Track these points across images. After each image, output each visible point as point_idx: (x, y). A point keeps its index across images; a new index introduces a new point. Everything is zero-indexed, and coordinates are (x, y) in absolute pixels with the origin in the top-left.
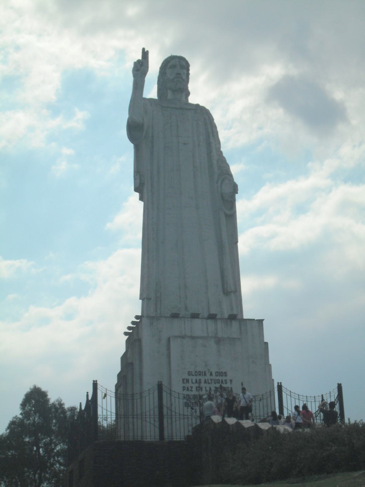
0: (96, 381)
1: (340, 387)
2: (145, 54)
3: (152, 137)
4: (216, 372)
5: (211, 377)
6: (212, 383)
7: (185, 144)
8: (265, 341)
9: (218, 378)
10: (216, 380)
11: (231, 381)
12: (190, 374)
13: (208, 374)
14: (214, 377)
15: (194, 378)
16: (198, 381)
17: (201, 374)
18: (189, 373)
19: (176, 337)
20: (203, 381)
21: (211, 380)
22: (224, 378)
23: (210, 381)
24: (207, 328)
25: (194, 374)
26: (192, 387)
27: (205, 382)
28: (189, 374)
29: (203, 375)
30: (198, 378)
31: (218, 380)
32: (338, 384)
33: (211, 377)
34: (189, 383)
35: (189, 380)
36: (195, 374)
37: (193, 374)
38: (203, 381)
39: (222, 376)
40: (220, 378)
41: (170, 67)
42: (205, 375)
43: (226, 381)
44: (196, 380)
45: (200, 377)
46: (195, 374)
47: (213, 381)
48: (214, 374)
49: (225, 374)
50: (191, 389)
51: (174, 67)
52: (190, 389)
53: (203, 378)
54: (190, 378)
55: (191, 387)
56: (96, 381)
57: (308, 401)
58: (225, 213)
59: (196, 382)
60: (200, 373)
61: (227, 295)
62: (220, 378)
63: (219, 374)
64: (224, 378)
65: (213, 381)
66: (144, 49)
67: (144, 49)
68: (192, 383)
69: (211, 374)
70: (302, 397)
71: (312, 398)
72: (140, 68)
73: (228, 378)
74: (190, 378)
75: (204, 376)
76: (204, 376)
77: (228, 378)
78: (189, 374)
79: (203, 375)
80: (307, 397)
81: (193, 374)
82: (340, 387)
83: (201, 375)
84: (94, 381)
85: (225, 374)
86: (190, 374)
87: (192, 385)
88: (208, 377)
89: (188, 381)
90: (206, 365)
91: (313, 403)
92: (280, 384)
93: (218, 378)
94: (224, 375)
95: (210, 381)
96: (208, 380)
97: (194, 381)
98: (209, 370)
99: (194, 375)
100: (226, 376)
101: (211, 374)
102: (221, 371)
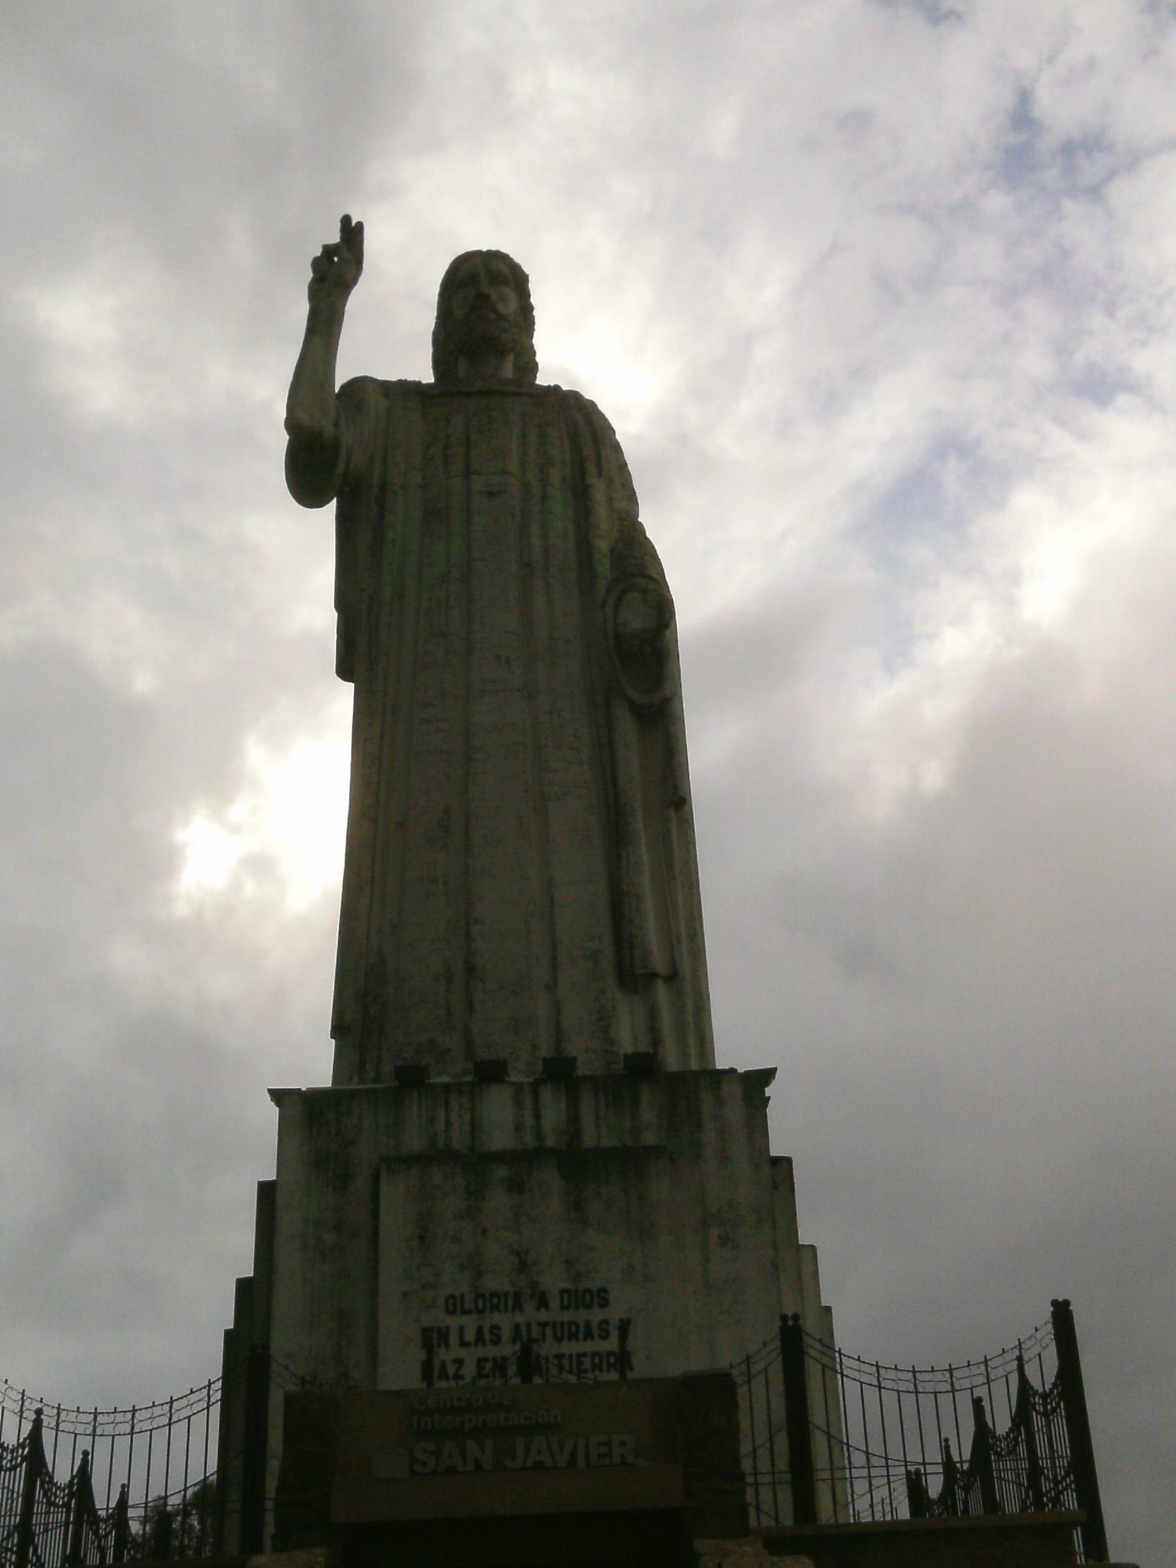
1: (1062, 1314)
3: (383, 488)
4: (564, 1292)
5: (543, 1316)
6: (544, 1339)
8: (776, 1150)
10: (562, 1324)
11: (624, 1327)
12: (454, 1305)
13: (529, 1306)
15: (470, 1324)
16: (487, 1336)
17: (498, 1305)
18: (451, 1301)
19: (405, 1161)
20: (506, 1335)
21: (543, 1325)
23: (536, 1332)
24: (537, 1116)
26: (460, 1362)
28: (451, 1308)
29: (510, 1308)
31: (571, 1323)
32: (1055, 1303)
33: (543, 1316)
34: (447, 1345)
35: (448, 1329)
36: (476, 1303)
38: (506, 1335)
39: (588, 1307)
40: (580, 1316)
43: (604, 1326)
44: (480, 1330)
45: (496, 1318)
46: (476, 1303)
47: (549, 1331)
48: (554, 1304)
49: (602, 1297)
50: (459, 1369)
52: (451, 1369)
53: (505, 1321)
54: (454, 1322)
55: (455, 1361)
57: (957, 1387)
59: (480, 1338)
60: (496, 1301)
62: (580, 1316)
63: (577, 1297)
64: (597, 1315)
65: (549, 1331)
66: (346, 220)
67: (346, 220)
68: (463, 1344)
70: (892, 1374)
75: (513, 1310)
76: (513, 1310)
78: (451, 1308)
79: (510, 1308)
80: (914, 1372)
81: (469, 1305)
82: (1062, 1314)
83: (502, 1307)
85: (602, 1297)
86: (454, 1304)
87: (463, 1353)
89: (444, 1335)
90: (523, 1267)
91: (945, 1400)
92: (790, 1323)
93: (568, 1316)
94: (596, 1300)
96: (529, 1326)
97: (470, 1336)
98: (533, 1285)
99: (469, 1312)
100: (605, 1303)
101: (542, 1303)
102: (582, 1286)
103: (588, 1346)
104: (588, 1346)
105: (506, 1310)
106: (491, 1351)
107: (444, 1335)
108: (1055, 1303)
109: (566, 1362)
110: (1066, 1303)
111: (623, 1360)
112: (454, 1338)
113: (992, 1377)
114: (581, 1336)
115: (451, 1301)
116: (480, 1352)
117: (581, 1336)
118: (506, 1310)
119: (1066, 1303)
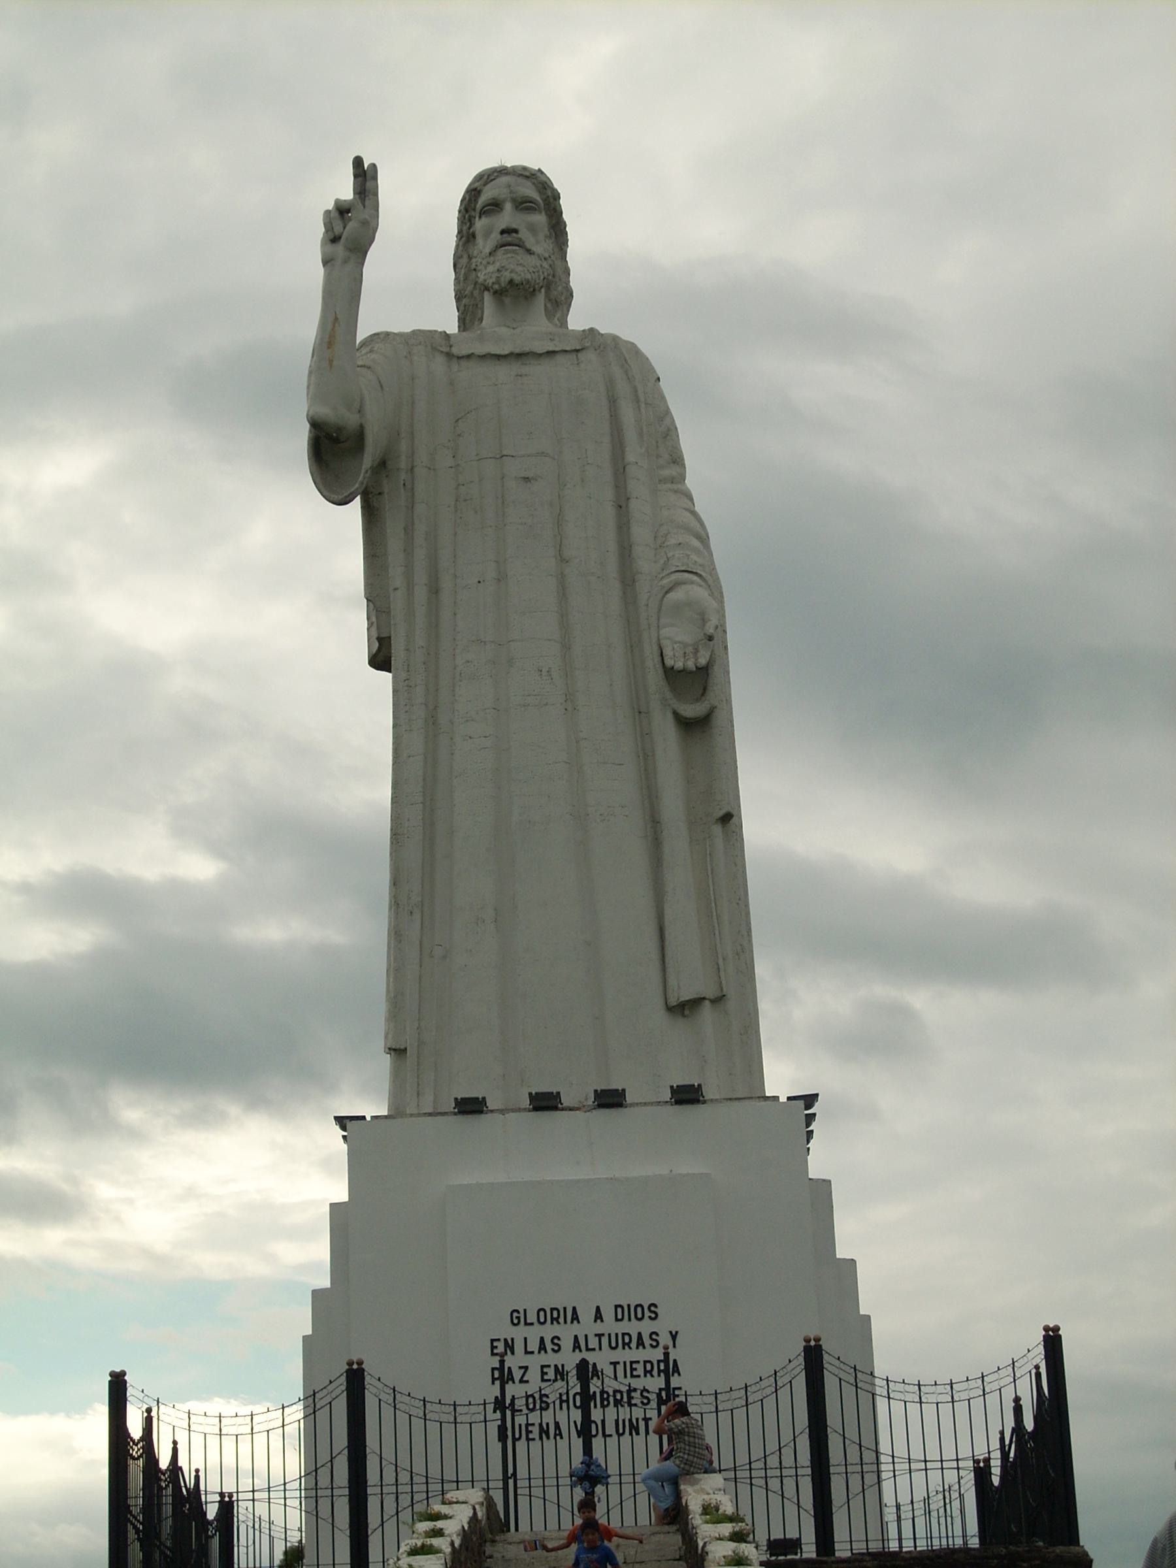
0: (123, 1373)
2: (365, 177)
5: (599, 1328)
7: (527, 479)
9: (622, 1327)
12: (517, 1318)
14: (610, 1326)
15: (534, 1334)
17: (557, 1319)
18: (515, 1314)
20: (567, 1344)
21: (600, 1336)
22: (646, 1327)
23: (593, 1342)
25: (535, 1320)
27: (576, 1346)
28: (516, 1321)
30: (548, 1331)
32: (1046, 1329)
33: (599, 1328)
37: (531, 1318)
38: (567, 1344)
40: (633, 1327)
41: (483, 213)
42: (575, 1318)
47: (605, 1340)
51: (495, 206)
53: (566, 1333)
54: (518, 1334)
56: (123, 1373)
58: (676, 714)
59: (542, 1347)
61: (684, 1016)
62: (633, 1327)
64: (646, 1327)
65: (605, 1340)
66: (358, 162)
67: (358, 162)
69: (598, 1316)
71: (972, 1384)
72: (350, 230)
73: (663, 1326)
74: (518, 1334)
77: (663, 1326)
78: (516, 1321)
81: (531, 1318)
83: (561, 1320)
84: (113, 1374)
86: (518, 1318)
88: (587, 1326)
89: (510, 1346)
93: (622, 1327)
94: (647, 1314)
95: (593, 1342)
97: (534, 1346)
101: (598, 1316)
103: (641, 1355)
104: (641, 1355)
105: (565, 1322)
106: (551, 1359)
107: (510, 1346)
108: (1046, 1329)
109: (620, 1368)
110: (1056, 1329)
111: (669, 1368)
112: (519, 1347)
113: (987, 1390)
114: (634, 1345)
115: (515, 1314)
116: (544, 1359)
117: (634, 1345)
118: (565, 1322)
119: (1056, 1329)
